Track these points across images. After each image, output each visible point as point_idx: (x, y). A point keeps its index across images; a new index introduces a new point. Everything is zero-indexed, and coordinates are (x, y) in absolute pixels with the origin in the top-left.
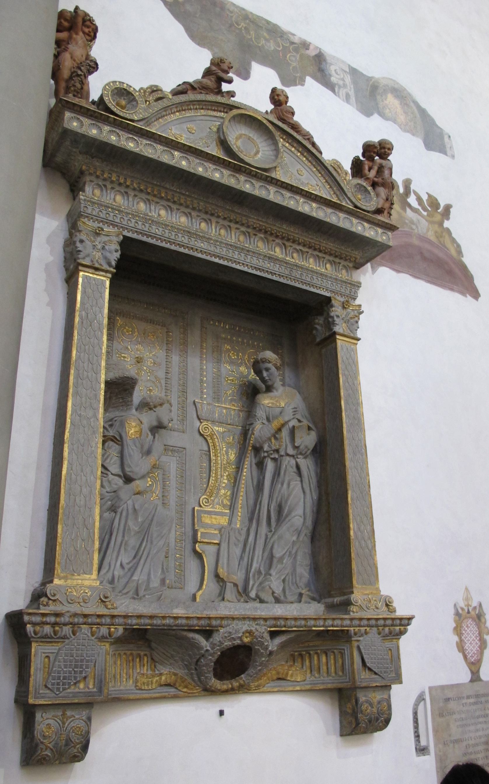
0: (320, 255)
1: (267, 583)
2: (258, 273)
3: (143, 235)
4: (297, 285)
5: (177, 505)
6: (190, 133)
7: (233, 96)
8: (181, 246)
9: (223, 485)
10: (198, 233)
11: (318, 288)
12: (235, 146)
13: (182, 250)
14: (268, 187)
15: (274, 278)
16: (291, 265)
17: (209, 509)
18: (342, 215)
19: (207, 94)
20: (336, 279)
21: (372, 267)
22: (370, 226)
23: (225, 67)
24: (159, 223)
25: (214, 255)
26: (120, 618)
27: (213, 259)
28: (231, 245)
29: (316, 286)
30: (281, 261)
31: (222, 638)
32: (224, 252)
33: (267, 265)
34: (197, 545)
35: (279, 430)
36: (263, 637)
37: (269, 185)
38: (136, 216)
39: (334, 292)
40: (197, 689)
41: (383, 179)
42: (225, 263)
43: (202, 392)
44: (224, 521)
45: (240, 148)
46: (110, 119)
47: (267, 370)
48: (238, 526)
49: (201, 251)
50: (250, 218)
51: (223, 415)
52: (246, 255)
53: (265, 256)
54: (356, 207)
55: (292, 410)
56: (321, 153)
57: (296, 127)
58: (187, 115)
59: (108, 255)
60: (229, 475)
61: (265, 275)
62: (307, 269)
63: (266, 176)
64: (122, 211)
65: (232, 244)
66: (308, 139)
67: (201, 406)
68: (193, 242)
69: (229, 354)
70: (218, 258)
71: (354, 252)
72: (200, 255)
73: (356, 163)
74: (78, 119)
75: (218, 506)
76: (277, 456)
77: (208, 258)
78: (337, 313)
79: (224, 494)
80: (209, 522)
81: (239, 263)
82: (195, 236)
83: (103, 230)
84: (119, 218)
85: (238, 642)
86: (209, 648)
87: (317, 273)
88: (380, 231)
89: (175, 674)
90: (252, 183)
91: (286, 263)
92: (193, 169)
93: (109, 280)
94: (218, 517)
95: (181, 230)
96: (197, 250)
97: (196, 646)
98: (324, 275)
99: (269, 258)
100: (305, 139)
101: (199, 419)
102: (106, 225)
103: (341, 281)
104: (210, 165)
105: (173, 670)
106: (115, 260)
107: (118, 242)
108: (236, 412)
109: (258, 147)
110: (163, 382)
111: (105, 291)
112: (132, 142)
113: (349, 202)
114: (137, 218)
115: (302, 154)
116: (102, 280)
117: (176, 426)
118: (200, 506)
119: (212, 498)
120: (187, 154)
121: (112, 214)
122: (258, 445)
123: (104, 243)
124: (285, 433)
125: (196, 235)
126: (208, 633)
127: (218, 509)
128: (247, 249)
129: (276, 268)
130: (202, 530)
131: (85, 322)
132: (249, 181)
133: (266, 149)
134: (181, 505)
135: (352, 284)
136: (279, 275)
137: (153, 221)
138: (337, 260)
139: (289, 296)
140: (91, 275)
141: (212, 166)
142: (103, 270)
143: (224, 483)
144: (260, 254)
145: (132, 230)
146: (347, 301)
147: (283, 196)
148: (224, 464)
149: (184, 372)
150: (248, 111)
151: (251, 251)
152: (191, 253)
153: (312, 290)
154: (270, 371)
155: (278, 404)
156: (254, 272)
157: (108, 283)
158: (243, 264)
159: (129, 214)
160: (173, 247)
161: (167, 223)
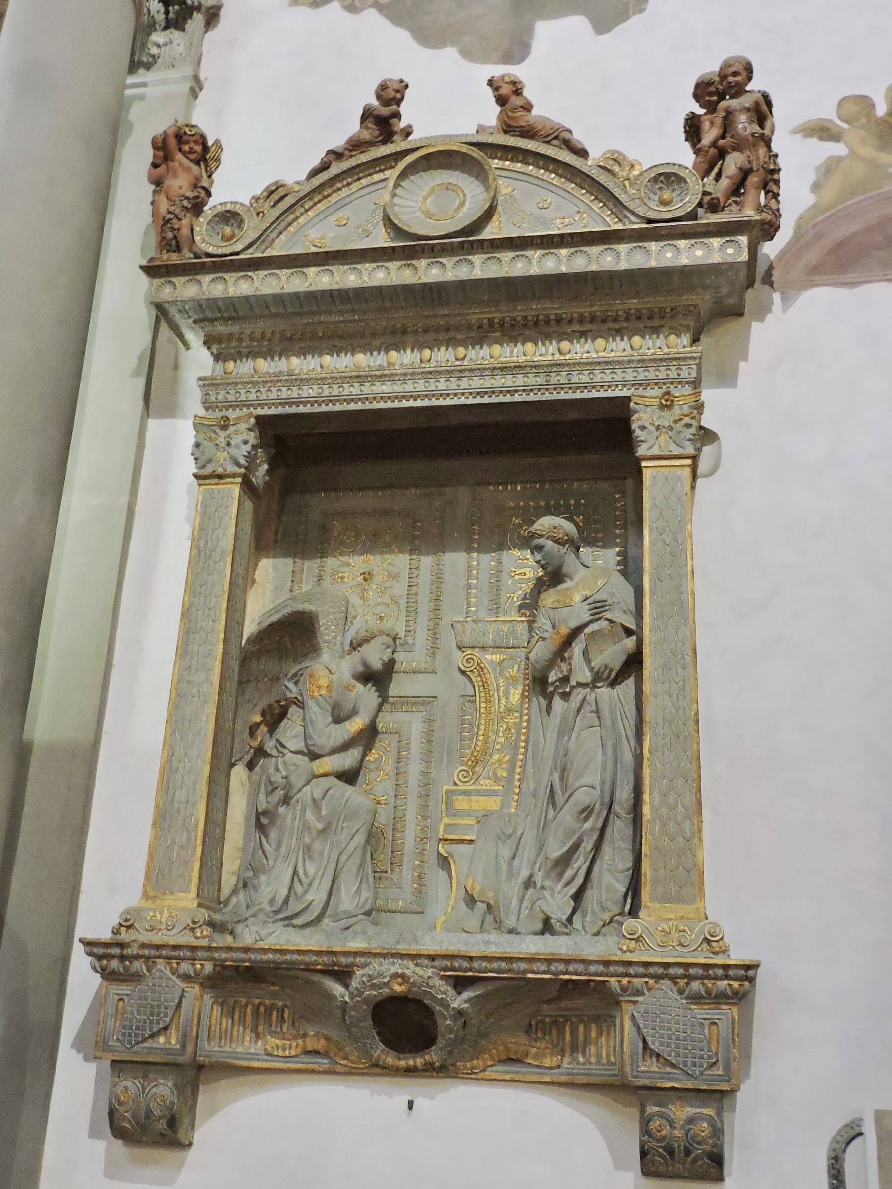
0: (617, 326)
1: (538, 902)
2: (486, 400)
3: (290, 404)
4: (563, 396)
5: (419, 786)
6: (340, 226)
7: (408, 134)
8: (349, 401)
9: (498, 747)
10: (374, 373)
11: (606, 388)
12: (419, 214)
13: (352, 407)
14: (470, 257)
15: (517, 398)
16: (547, 366)
17: (470, 788)
18: (623, 248)
19: (363, 152)
20: (643, 361)
21: (783, 299)
22: (693, 241)
23: (391, 93)
24: (311, 379)
25: (404, 397)
26: (185, 951)
27: (405, 404)
28: (430, 372)
29: (602, 387)
30: (525, 366)
31: (359, 983)
32: (421, 386)
33: (498, 382)
34: (440, 845)
35: (568, 642)
36: (428, 984)
37: (470, 254)
38: (277, 381)
39: (641, 385)
40: (364, 1063)
41: (732, 137)
42: (426, 403)
43: (468, 604)
44: (492, 804)
45: (428, 212)
46: (208, 264)
47: (539, 548)
48: (513, 810)
49: (382, 398)
50: (468, 314)
51: (501, 633)
52: (459, 379)
53: (494, 368)
54: (650, 221)
55: (588, 607)
56: (582, 153)
57: (528, 133)
58: (334, 201)
59: (233, 451)
60: (509, 729)
61: (502, 399)
62: (579, 364)
63: (460, 242)
64: (257, 382)
65: (432, 369)
66: (556, 138)
67: (463, 626)
68: (367, 389)
69: (520, 532)
70: (412, 400)
71: (686, 297)
72: (382, 405)
73: (690, 127)
74: (170, 282)
75: (487, 782)
76: (568, 689)
77: (396, 404)
78: (640, 423)
79: (498, 760)
80: (467, 808)
81: (448, 395)
82: (369, 379)
83: (228, 419)
84: (253, 393)
85: (386, 991)
86: (347, 999)
87: (599, 363)
88: (716, 242)
89: (327, 1039)
90: (441, 263)
91: (535, 367)
92: (337, 283)
93: (239, 485)
94: (481, 798)
95: (347, 377)
96: (374, 398)
97: (328, 996)
98: (613, 361)
99: (502, 369)
100: (548, 142)
101: (460, 648)
102: (238, 409)
103: (655, 360)
104: (367, 265)
105: (324, 1031)
106: (244, 456)
107: (250, 429)
108: (526, 624)
109: (465, 196)
110: (403, 603)
111: (233, 503)
112: (245, 283)
113: (633, 219)
114: (280, 384)
115: (547, 170)
116: (229, 490)
117: (423, 665)
118: (456, 784)
119: (477, 769)
120: (328, 264)
121: (243, 392)
122: (538, 676)
123: (229, 437)
124: (577, 648)
125: (371, 376)
126: (343, 975)
127: (485, 784)
128: (459, 368)
129: (520, 380)
130: (446, 820)
131: (202, 554)
132: (437, 262)
133: (478, 192)
134: (427, 785)
135: (679, 359)
136: (524, 390)
137: (301, 380)
138: (656, 322)
139: (574, 415)
140: (214, 487)
141: (368, 266)
142: (228, 476)
143: (499, 743)
144: (485, 369)
145: (273, 404)
146: (668, 393)
147: (500, 261)
148: (501, 713)
149: (438, 577)
150: (434, 146)
151: (466, 370)
152: (367, 406)
153: (594, 394)
154: (544, 549)
155: (567, 602)
156: (479, 400)
157: (236, 490)
158: (456, 395)
159: (266, 382)
160: (338, 407)
161: (324, 375)
